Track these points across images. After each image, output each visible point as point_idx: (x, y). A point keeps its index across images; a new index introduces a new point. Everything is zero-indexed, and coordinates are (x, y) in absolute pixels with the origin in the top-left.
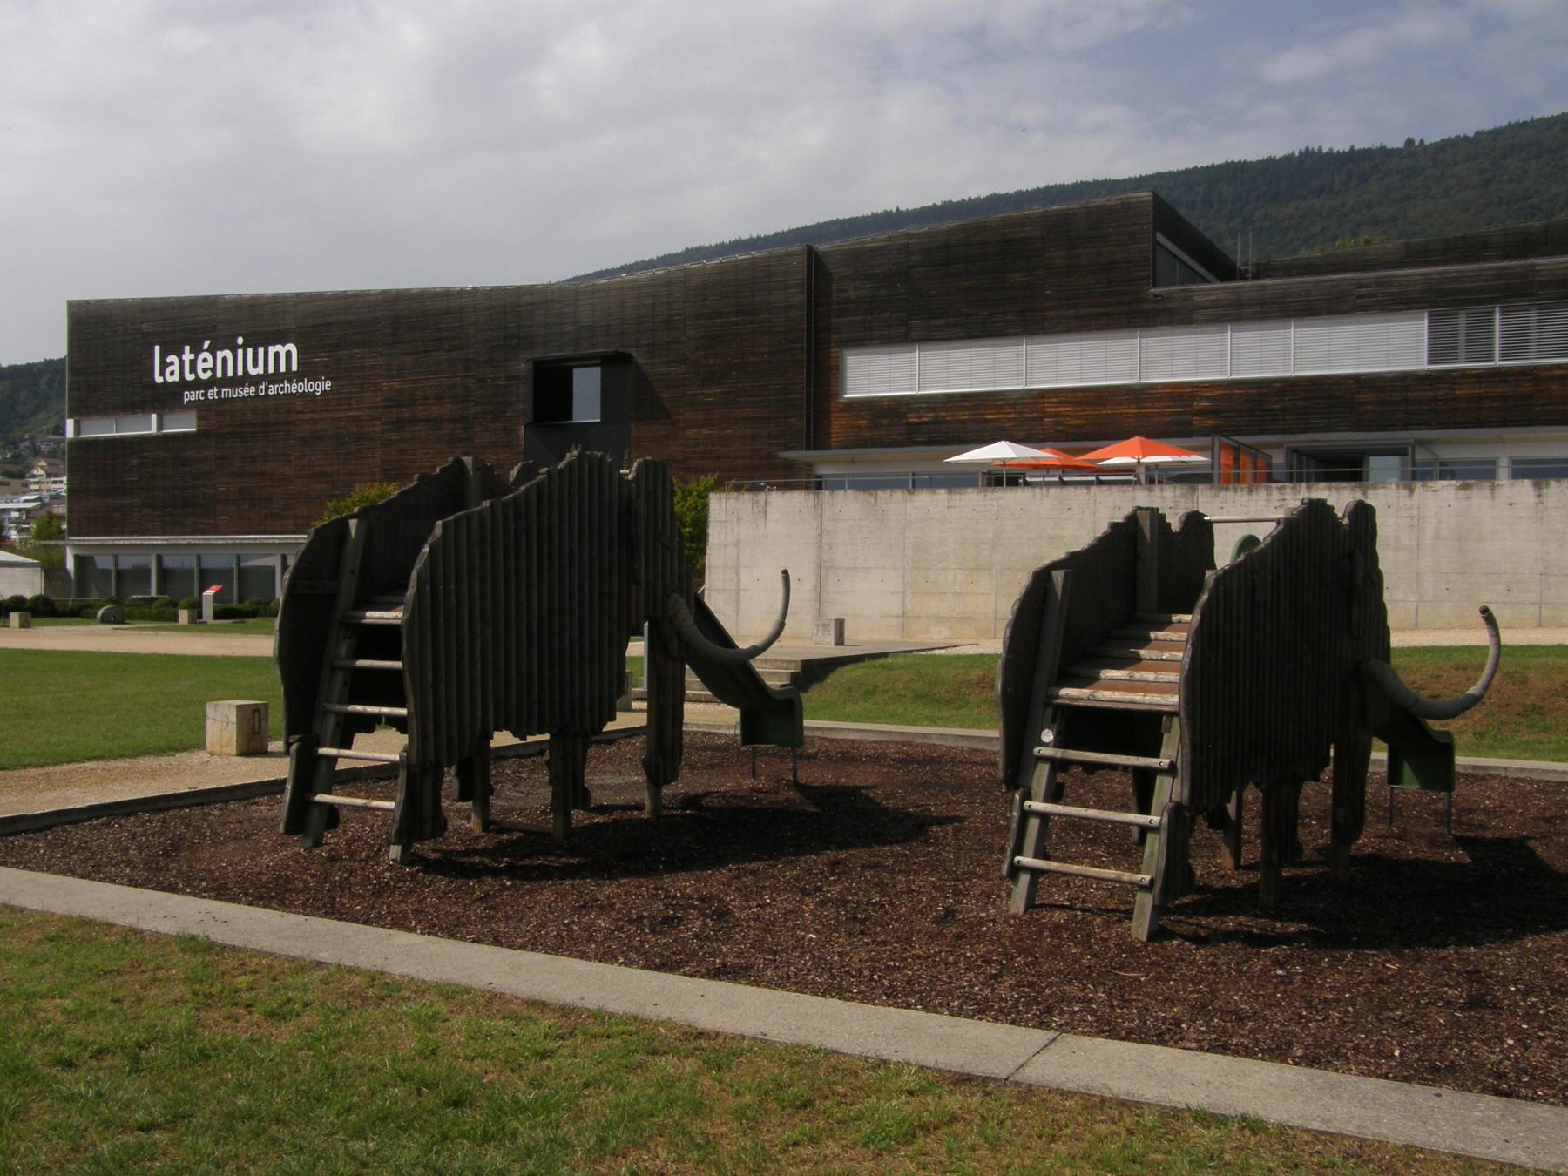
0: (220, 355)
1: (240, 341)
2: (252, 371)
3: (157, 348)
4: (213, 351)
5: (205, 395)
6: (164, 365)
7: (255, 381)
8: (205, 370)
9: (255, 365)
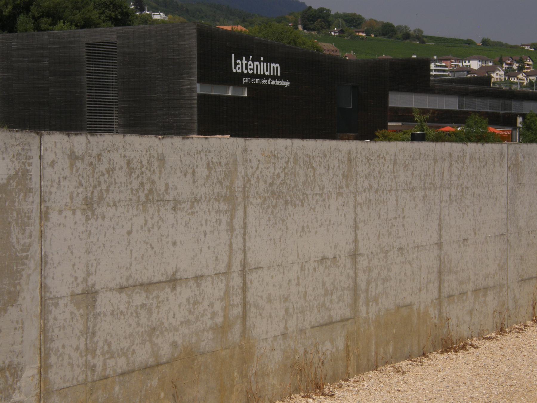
1: (262, 59)
3: (233, 55)
4: (253, 61)
5: (251, 80)
6: (236, 64)
7: (267, 77)
8: (250, 69)
9: (267, 71)
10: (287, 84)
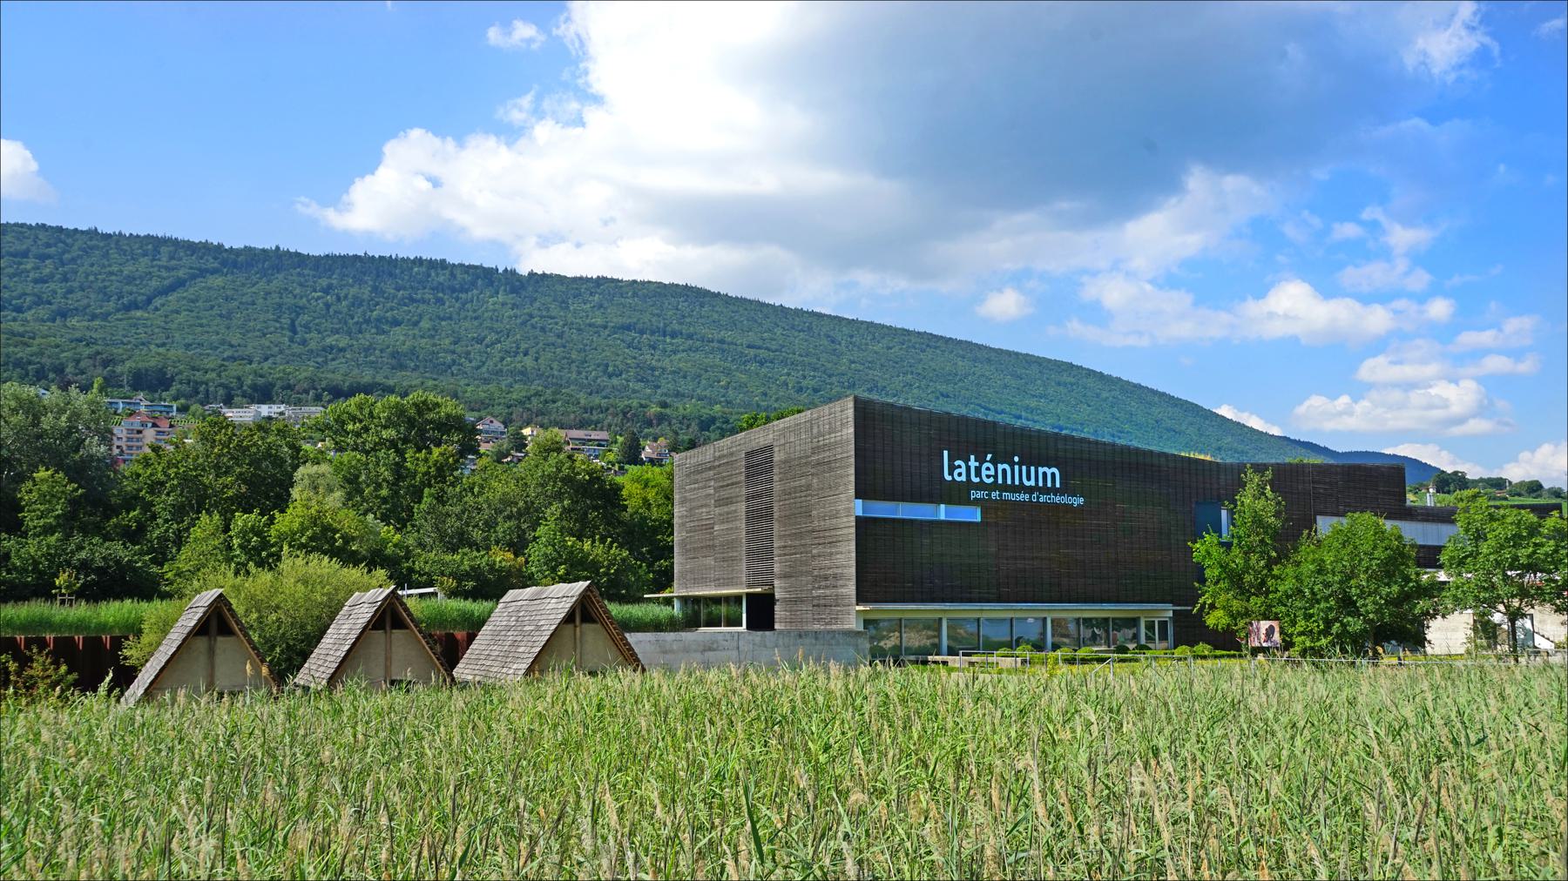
0: (1000, 467)
1: (1016, 459)
2: (1027, 483)
6: (952, 469)
7: (1030, 490)
9: (1029, 479)
10: (1078, 501)
